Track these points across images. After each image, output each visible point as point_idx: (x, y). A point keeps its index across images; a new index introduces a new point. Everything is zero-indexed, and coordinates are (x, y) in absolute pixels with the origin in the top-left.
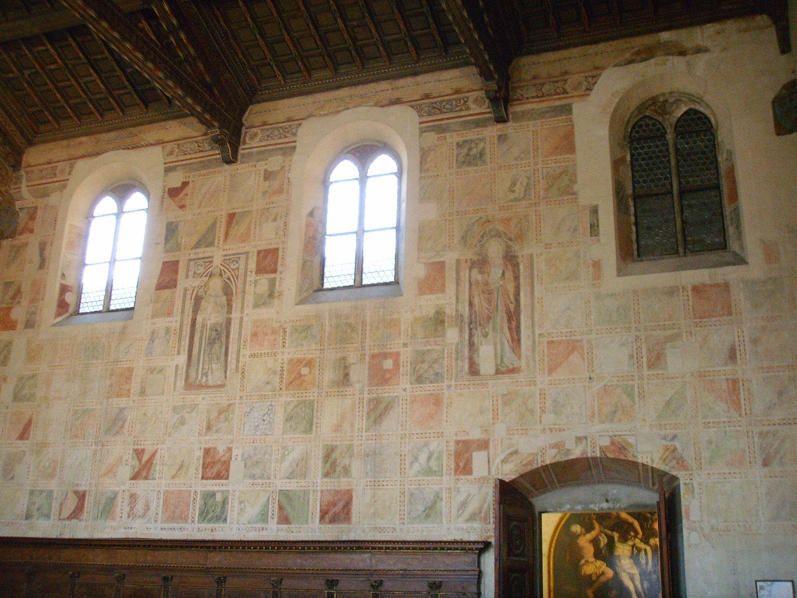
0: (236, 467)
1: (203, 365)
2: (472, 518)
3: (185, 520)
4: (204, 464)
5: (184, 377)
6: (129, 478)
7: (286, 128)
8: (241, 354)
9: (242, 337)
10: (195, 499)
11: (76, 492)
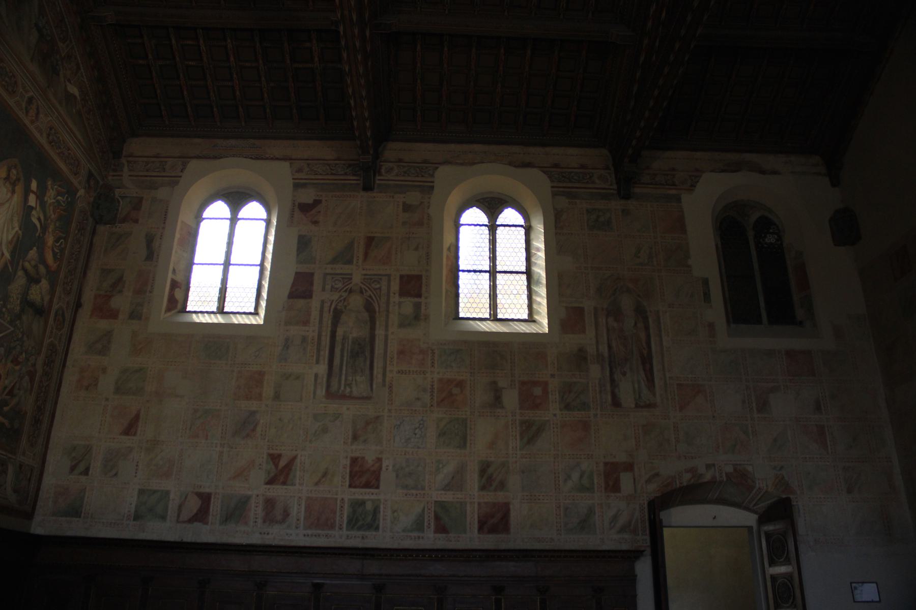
0: (387, 477)
1: (346, 377)
2: (622, 530)
3: (332, 527)
4: (351, 472)
7: (422, 169)
8: (388, 369)
10: (342, 507)
11: (200, 495)
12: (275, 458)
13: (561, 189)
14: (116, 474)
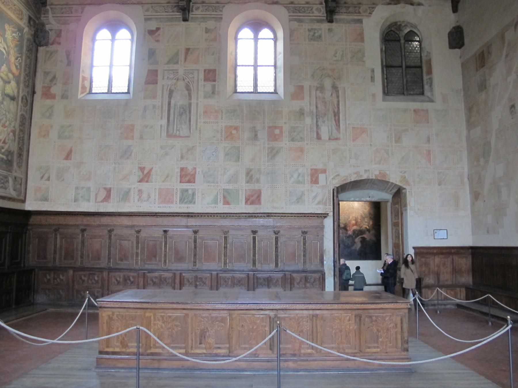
0: (199, 177)
4: (180, 175)
5: (166, 131)
6: (137, 182)
7: (216, 7)
9: (198, 113)
10: (176, 193)
11: (105, 189)
12: (142, 169)
13: (294, 17)
14: (63, 180)
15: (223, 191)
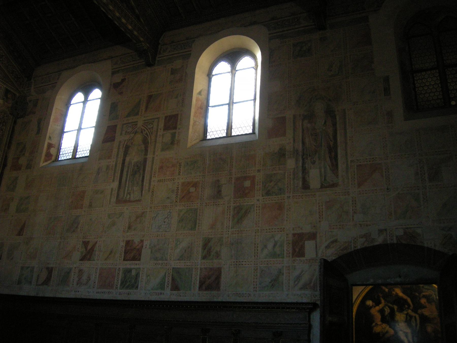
0: (146, 253)
1: (128, 188)
2: (304, 287)
4: (125, 250)
9: (153, 169)
10: (118, 274)
11: (48, 268)
12: (86, 244)
13: (275, 34)
15: (173, 271)
